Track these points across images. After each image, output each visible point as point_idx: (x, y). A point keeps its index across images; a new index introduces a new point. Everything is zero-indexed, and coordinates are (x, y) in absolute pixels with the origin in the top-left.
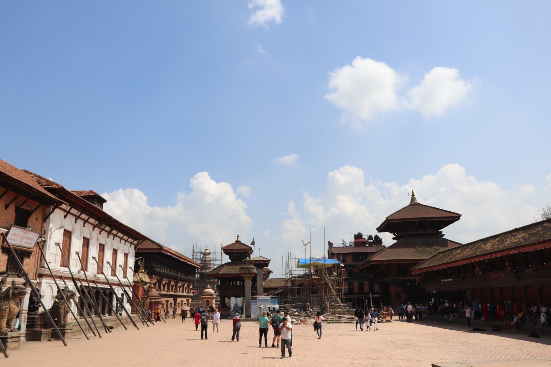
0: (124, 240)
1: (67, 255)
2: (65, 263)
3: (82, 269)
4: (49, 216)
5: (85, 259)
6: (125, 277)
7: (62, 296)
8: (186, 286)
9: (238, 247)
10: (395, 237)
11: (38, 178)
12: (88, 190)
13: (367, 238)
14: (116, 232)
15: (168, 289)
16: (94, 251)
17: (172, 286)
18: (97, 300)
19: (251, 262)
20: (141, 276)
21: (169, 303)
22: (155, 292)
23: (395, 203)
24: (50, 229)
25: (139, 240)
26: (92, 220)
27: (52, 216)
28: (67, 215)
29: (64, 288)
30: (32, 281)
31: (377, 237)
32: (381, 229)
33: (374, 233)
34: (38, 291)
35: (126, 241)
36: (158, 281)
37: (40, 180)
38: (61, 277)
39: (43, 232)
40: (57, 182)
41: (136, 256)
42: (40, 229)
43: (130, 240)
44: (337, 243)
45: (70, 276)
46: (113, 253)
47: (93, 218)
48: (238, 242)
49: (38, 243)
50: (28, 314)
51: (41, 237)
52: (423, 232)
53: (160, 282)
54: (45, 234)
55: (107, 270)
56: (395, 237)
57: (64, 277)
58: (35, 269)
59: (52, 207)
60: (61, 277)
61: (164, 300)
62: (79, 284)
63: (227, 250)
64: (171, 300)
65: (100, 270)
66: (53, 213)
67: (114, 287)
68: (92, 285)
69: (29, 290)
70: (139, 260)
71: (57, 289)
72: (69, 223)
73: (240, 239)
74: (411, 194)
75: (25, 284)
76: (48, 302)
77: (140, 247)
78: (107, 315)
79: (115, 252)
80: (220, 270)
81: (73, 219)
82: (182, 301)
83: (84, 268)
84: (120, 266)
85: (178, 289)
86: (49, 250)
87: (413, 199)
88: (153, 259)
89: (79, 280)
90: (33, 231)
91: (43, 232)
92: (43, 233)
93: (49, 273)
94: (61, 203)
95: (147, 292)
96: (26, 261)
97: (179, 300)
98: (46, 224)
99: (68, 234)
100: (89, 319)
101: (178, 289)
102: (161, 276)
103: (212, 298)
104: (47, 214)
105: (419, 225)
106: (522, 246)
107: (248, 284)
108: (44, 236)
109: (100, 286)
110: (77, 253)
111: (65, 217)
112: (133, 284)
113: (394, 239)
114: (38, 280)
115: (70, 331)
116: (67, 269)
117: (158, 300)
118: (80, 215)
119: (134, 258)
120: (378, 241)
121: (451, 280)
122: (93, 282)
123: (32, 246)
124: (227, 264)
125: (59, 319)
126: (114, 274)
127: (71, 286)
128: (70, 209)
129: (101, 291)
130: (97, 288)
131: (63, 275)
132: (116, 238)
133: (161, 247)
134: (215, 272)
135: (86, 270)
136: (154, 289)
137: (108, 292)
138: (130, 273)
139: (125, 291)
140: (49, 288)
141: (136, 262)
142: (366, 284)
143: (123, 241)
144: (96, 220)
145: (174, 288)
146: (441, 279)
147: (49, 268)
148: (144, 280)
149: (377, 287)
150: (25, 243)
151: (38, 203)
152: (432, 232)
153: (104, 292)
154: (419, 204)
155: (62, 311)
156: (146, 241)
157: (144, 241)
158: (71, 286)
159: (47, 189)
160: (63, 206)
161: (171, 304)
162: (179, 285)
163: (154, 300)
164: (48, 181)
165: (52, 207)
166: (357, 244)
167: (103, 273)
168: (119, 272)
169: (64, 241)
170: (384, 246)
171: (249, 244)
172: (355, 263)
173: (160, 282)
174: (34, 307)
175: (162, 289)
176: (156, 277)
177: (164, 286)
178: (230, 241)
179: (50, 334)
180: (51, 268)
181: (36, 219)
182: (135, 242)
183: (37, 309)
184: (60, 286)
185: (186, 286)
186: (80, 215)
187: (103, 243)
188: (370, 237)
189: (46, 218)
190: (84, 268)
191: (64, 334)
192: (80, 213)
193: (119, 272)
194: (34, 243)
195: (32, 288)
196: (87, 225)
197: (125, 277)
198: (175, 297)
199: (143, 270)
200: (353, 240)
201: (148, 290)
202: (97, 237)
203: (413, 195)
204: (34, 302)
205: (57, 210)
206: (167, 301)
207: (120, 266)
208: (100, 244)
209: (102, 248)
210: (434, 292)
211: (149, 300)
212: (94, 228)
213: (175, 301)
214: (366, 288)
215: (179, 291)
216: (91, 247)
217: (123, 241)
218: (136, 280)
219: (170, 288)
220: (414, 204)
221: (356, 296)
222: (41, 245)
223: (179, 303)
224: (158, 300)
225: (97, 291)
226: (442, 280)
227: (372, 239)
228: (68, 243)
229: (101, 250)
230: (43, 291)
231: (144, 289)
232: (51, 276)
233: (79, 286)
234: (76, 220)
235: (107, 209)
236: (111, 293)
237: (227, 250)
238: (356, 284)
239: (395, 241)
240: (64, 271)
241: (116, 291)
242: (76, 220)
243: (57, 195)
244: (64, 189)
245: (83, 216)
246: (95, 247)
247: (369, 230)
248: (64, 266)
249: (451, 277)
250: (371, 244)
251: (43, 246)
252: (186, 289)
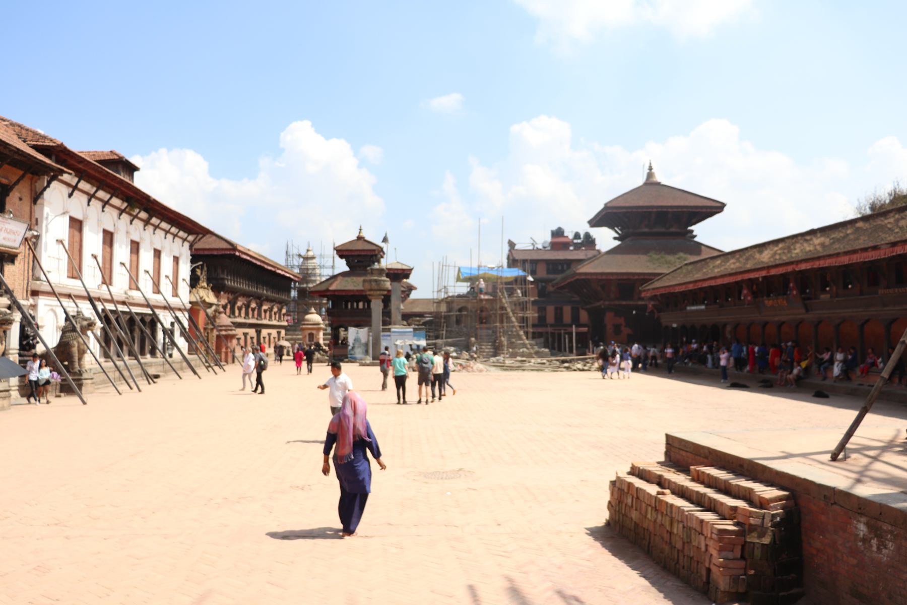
0: (172, 234)
1: (78, 258)
2: (75, 272)
3: (104, 282)
4: (42, 193)
5: (108, 266)
6: (175, 294)
7: (72, 328)
8: (275, 309)
9: (360, 246)
10: (617, 236)
11: (17, 129)
12: (107, 149)
13: (571, 236)
14: (158, 221)
15: (247, 314)
16: (122, 252)
17: (253, 310)
18: (133, 332)
19: (381, 271)
22: (224, 320)
23: (620, 181)
24: (45, 215)
25: (197, 234)
26: (116, 201)
27: (47, 194)
28: (73, 192)
29: (75, 314)
30: (22, 302)
31: (587, 235)
32: (596, 222)
33: (584, 228)
34: (33, 318)
35: (175, 236)
36: (229, 302)
37: (21, 131)
38: (69, 296)
39: (34, 221)
40: (51, 135)
41: (193, 261)
42: (27, 216)
43: (181, 234)
44: (523, 244)
45: (85, 294)
46: (155, 256)
47: (117, 197)
48: (360, 238)
49: (26, 239)
50: (20, 355)
51: (30, 229)
52: (663, 230)
53: (232, 303)
54: (37, 224)
55: (146, 283)
56: (617, 236)
57: (76, 296)
58: (26, 282)
59: (46, 178)
60: (69, 296)
61: (239, 332)
62: (100, 307)
63: (342, 252)
64: (252, 332)
65: (134, 284)
66: (48, 190)
67: (157, 311)
68: (121, 308)
69: (17, 317)
70: (197, 267)
71: (64, 316)
72: (78, 205)
73: (363, 234)
74: (647, 167)
75: (9, 308)
76: (50, 336)
77: (199, 245)
78: (148, 356)
79: (157, 253)
80: (331, 284)
81: (85, 198)
82: (269, 334)
83: (107, 280)
84: (167, 277)
85: (263, 314)
86: (46, 250)
87: (650, 175)
88: (221, 266)
89: (99, 299)
90: (16, 218)
91: (34, 221)
92: (33, 223)
93: (49, 289)
94: (62, 172)
95: (212, 320)
96: (8, 268)
97: (265, 332)
98: (37, 208)
99: (76, 225)
100: (118, 363)
101: (263, 314)
102: (235, 294)
103: (319, 329)
104: (39, 191)
105: (659, 219)
106: (819, 258)
107: (377, 306)
108: (36, 228)
109: (135, 310)
110: (95, 257)
111: (70, 195)
112: (189, 306)
113: (615, 238)
114: (31, 301)
115: (89, 381)
116: (77, 283)
117: (230, 333)
118: (96, 192)
119: (189, 264)
120: (589, 242)
121: (703, 307)
122: (124, 303)
123: (17, 245)
124: (344, 274)
125: (71, 362)
126: (157, 290)
127: (87, 310)
128: (78, 182)
129: (138, 318)
130: (130, 313)
131: (73, 293)
132: (158, 231)
133: (234, 247)
134: (323, 288)
135: (111, 284)
136: (223, 315)
137: (148, 319)
138: (184, 288)
139: (177, 318)
140: (51, 314)
141: (193, 271)
142: (567, 310)
143: (170, 237)
144: (123, 200)
145: (256, 312)
146: (687, 305)
147: (48, 281)
148: (207, 300)
149: (584, 316)
150: (4, 239)
151: (21, 172)
152: (678, 230)
153: (142, 320)
154: (659, 184)
155: (75, 350)
156: (208, 236)
157: (204, 236)
158: (87, 310)
159: (35, 147)
160: (66, 177)
161: (252, 338)
162: (265, 307)
163: (224, 333)
164: (35, 133)
165: (46, 178)
166: (555, 246)
167: (138, 289)
168: (166, 286)
169: (71, 237)
170: (599, 251)
171: (378, 241)
172: (551, 276)
173: (232, 303)
174: (28, 344)
176: (226, 295)
177: (240, 309)
178: (347, 236)
179: (58, 387)
180: (51, 281)
181: (20, 199)
182: (191, 238)
183: (34, 347)
184: (68, 310)
185: (275, 309)
186: (96, 192)
187: (137, 239)
188: (577, 236)
189: (36, 197)
190: (107, 280)
191: (80, 386)
192: (95, 189)
194: (19, 239)
195: (23, 313)
196: (107, 208)
197: (175, 294)
198: (258, 327)
199: (205, 284)
200: (548, 238)
201: (214, 317)
202: (127, 229)
203: (651, 169)
204: (27, 337)
205: (55, 184)
206: (245, 334)
207: (167, 277)
208: (132, 242)
209: (135, 247)
210: (675, 325)
211: (215, 333)
212: (120, 214)
213: (259, 333)
214: (567, 317)
215: (265, 318)
216: (116, 246)
217: (170, 237)
218: (194, 300)
219: (250, 312)
220: (651, 183)
221: (550, 329)
222: (33, 243)
223: (264, 338)
226: (688, 308)
227: (580, 238)
228: (77, 239)
229: (135, 250)
231: (207, 315)
232: (53, 293)
233: (100, 311)
234: (89, 201)
235: (140, 182)
236: (153, 322)
237: (342, 252)
238: (550, 309)
239: (617, 243)
240: (74, 286)
241: (161, 318)
242: (89, 201)
243: (54, 157)
244: (65, 148)
245: (101, 194)
246: (124, 247)
247: (576, 223)
248: (73, 278)
249: (702, 303)
250: (577, 247)
251: (35, 244)
252: (275, 314)
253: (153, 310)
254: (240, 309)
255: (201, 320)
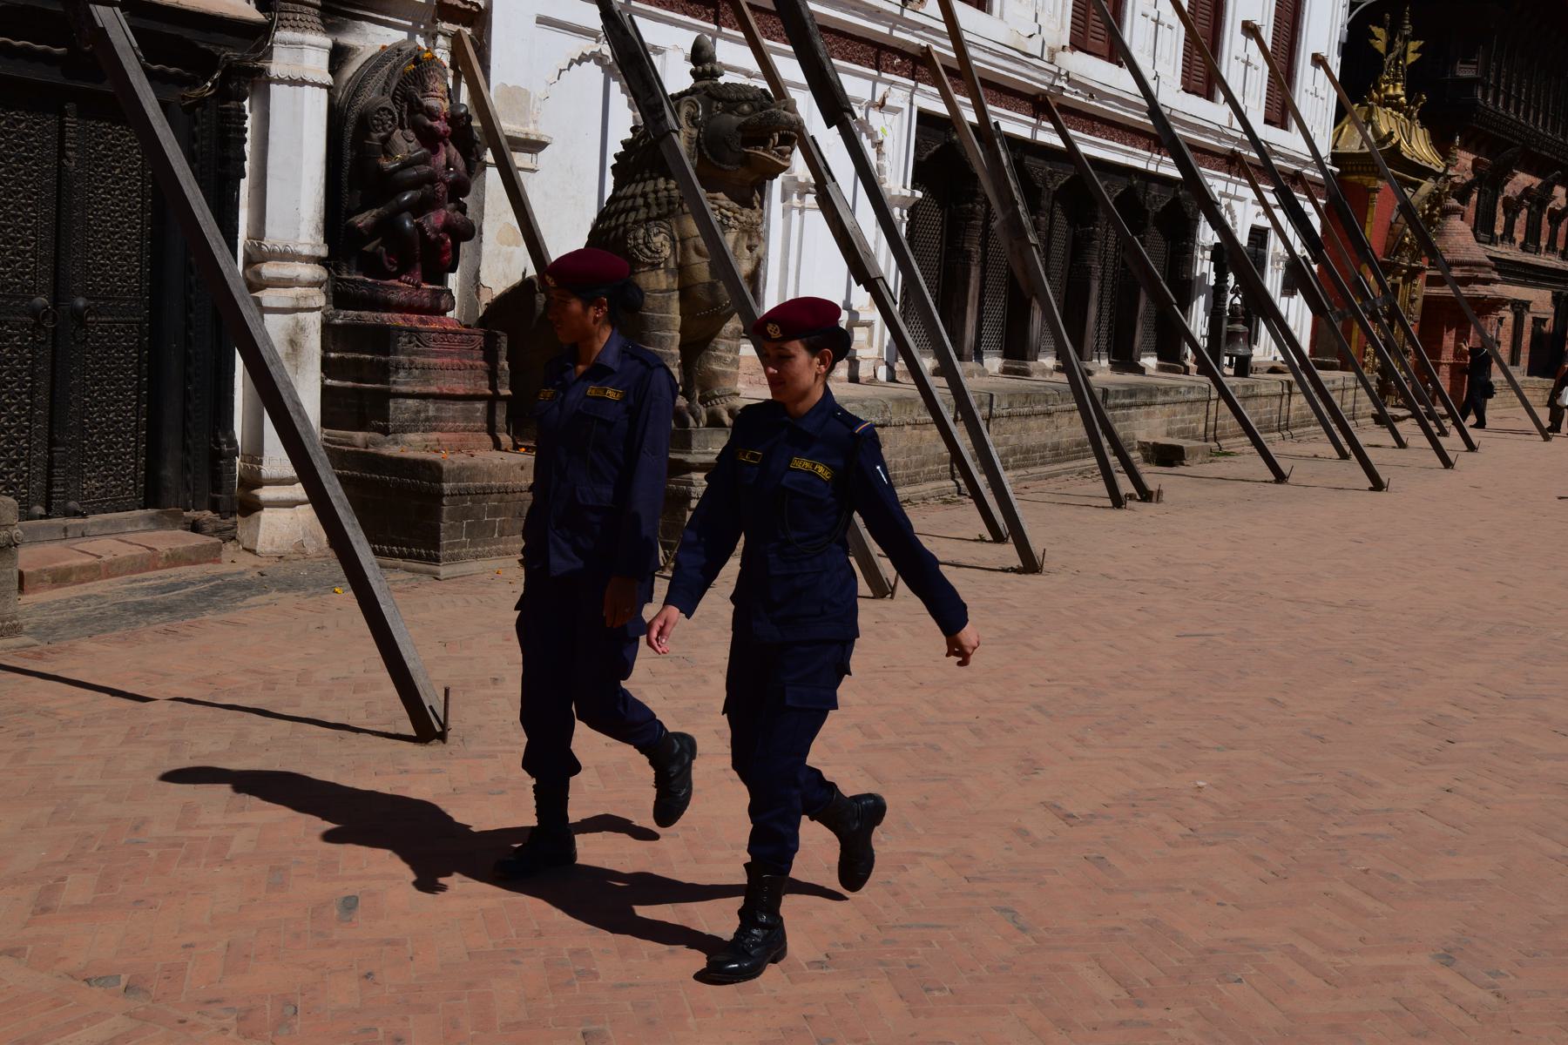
20: (1386, 121)
21: (1528, 319)
22: (1459, 237)
50: (340, 297)
53: (1489, 179)
68: (1015, 124)
78: (1150, 362)
95: (1422, 229)
109: (1092, 147)
117: (1482, 290)
126: (1203, 75)
129: (1108, 192)
130: (1070, 153)
137: (1157, 201)
138: (1316, 96)
173: (1489, 179)
175: (1499, 231)
177: (1512, 208)
193: (1245, 68)
207: (1250, 30)
211: (1421, 289)
224: (1482, 290)
225: (1073, 188)
230: (518, 96)
231: (1406, 208)
253: (1182, 163)
254: (1512, 208)
255: (1380, 220)
